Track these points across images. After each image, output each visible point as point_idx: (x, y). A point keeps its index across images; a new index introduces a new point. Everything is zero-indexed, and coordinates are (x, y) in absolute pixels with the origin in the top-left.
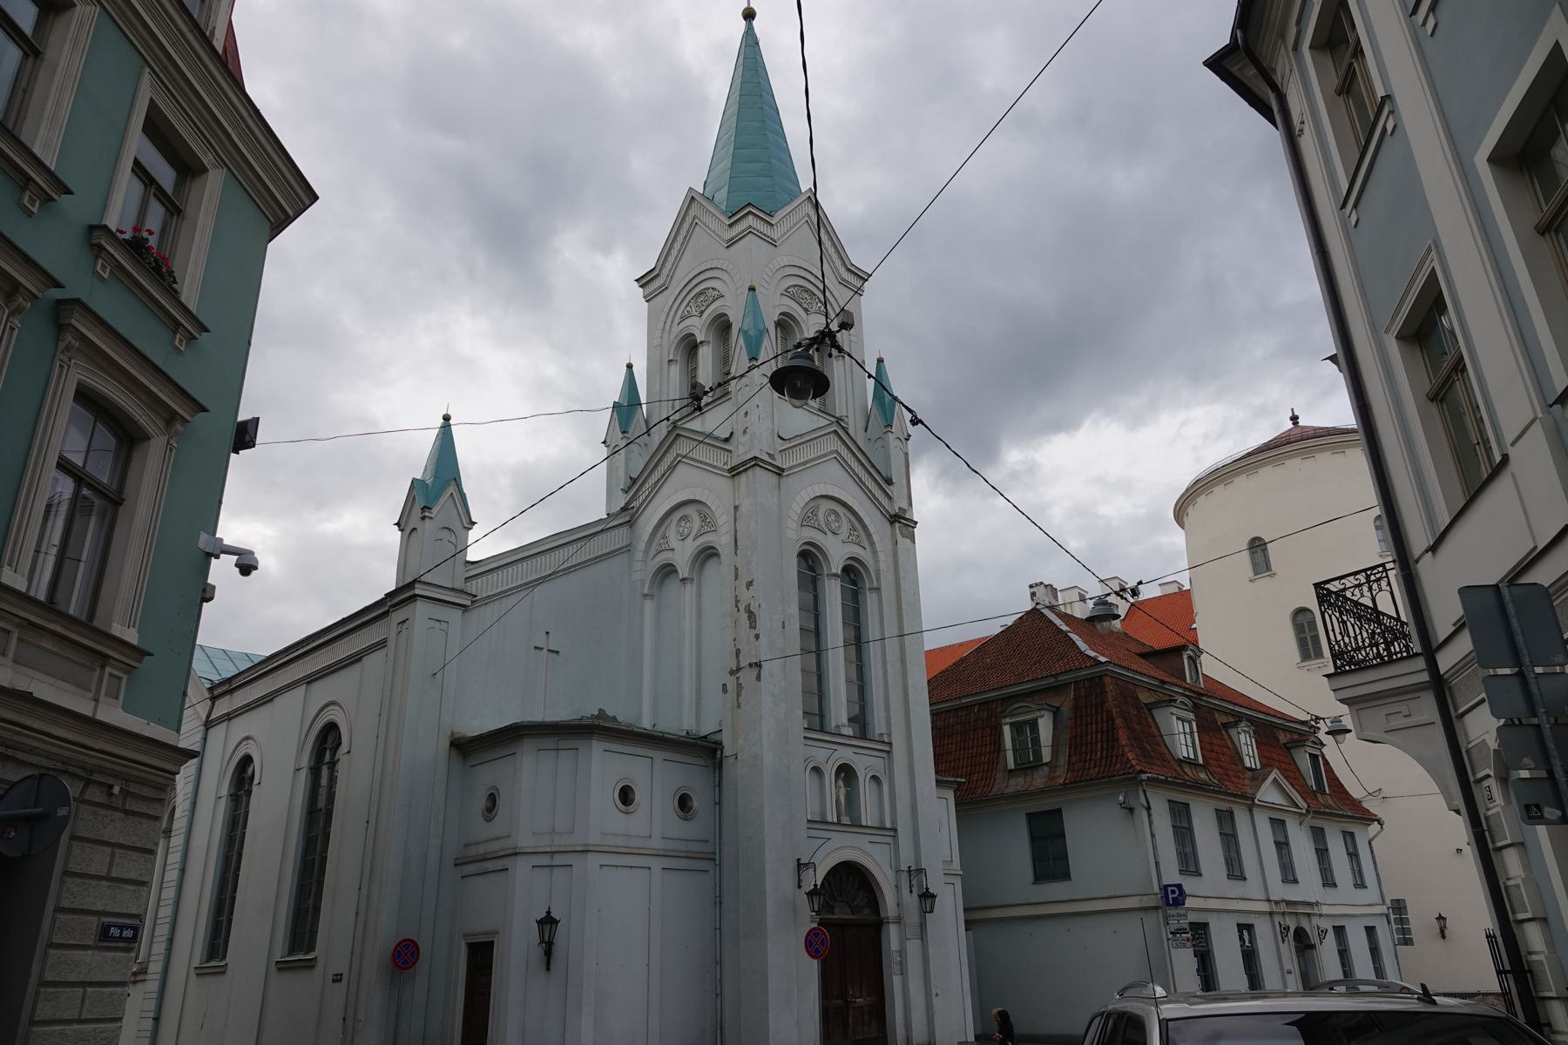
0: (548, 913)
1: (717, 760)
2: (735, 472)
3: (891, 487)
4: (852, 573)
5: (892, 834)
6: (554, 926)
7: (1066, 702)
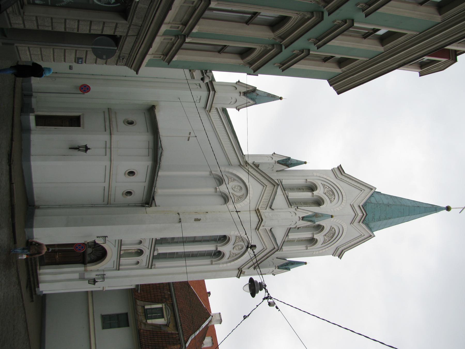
0: (89, 149)
1: (144, 205)
2: (257, 211)
3: (253, 269)
4: (218, 254)
5: (117, 269)
6: (85, 151)
7: (171, 330)
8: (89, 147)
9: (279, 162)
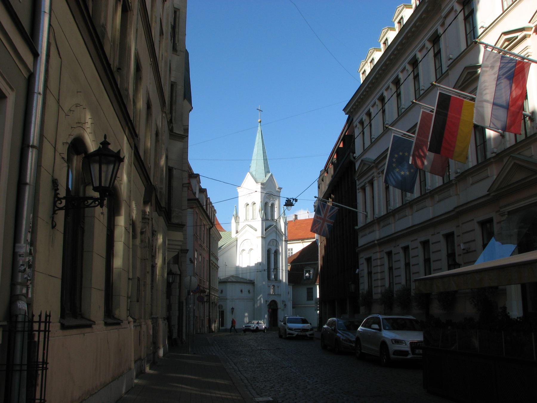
8: (232, 307)
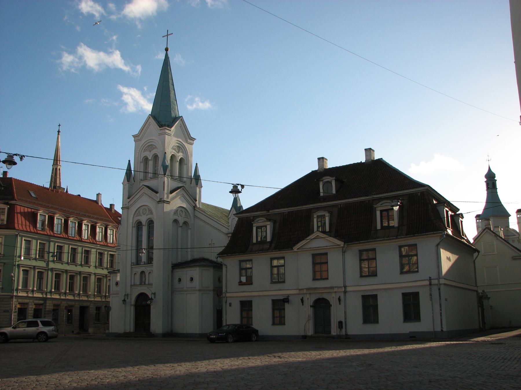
9: (128, 181)
